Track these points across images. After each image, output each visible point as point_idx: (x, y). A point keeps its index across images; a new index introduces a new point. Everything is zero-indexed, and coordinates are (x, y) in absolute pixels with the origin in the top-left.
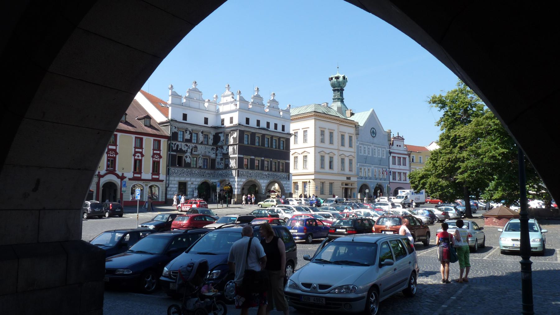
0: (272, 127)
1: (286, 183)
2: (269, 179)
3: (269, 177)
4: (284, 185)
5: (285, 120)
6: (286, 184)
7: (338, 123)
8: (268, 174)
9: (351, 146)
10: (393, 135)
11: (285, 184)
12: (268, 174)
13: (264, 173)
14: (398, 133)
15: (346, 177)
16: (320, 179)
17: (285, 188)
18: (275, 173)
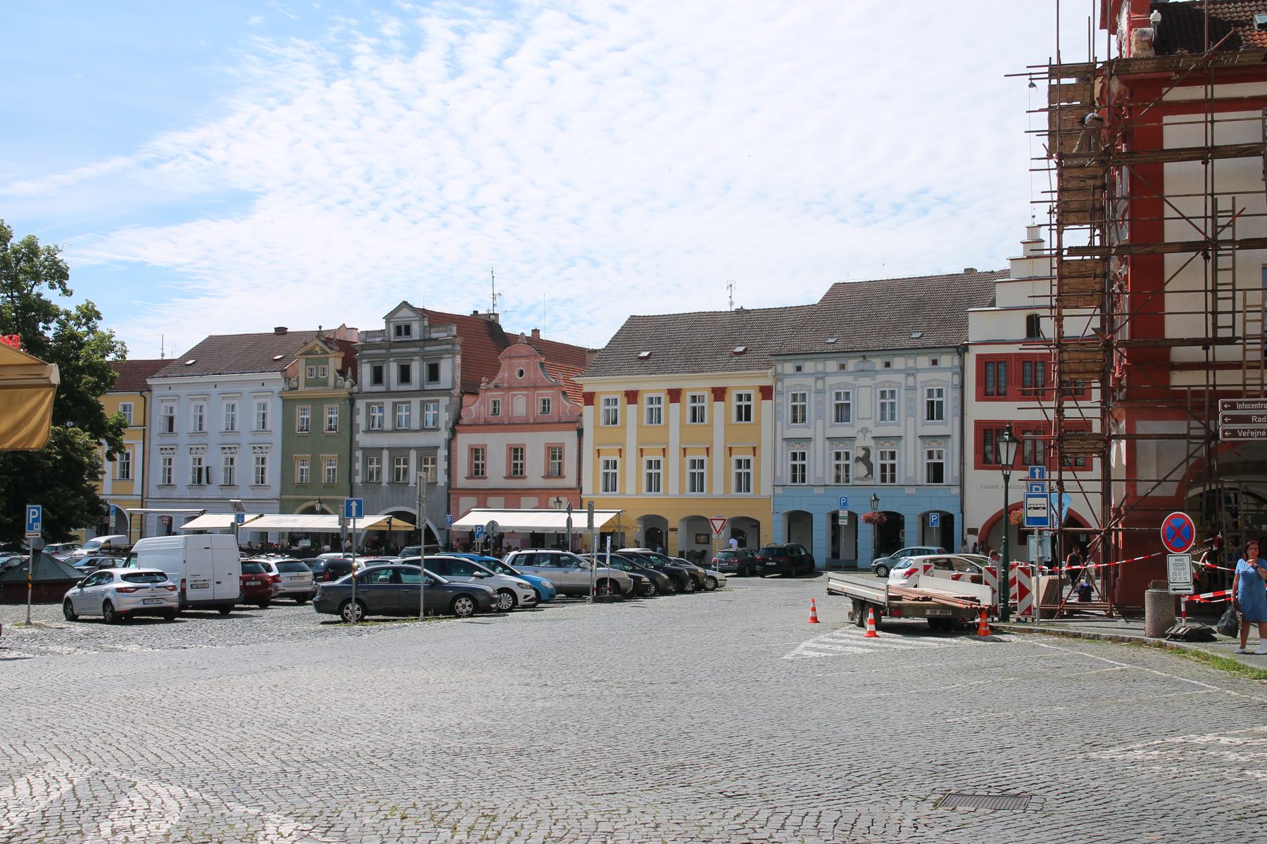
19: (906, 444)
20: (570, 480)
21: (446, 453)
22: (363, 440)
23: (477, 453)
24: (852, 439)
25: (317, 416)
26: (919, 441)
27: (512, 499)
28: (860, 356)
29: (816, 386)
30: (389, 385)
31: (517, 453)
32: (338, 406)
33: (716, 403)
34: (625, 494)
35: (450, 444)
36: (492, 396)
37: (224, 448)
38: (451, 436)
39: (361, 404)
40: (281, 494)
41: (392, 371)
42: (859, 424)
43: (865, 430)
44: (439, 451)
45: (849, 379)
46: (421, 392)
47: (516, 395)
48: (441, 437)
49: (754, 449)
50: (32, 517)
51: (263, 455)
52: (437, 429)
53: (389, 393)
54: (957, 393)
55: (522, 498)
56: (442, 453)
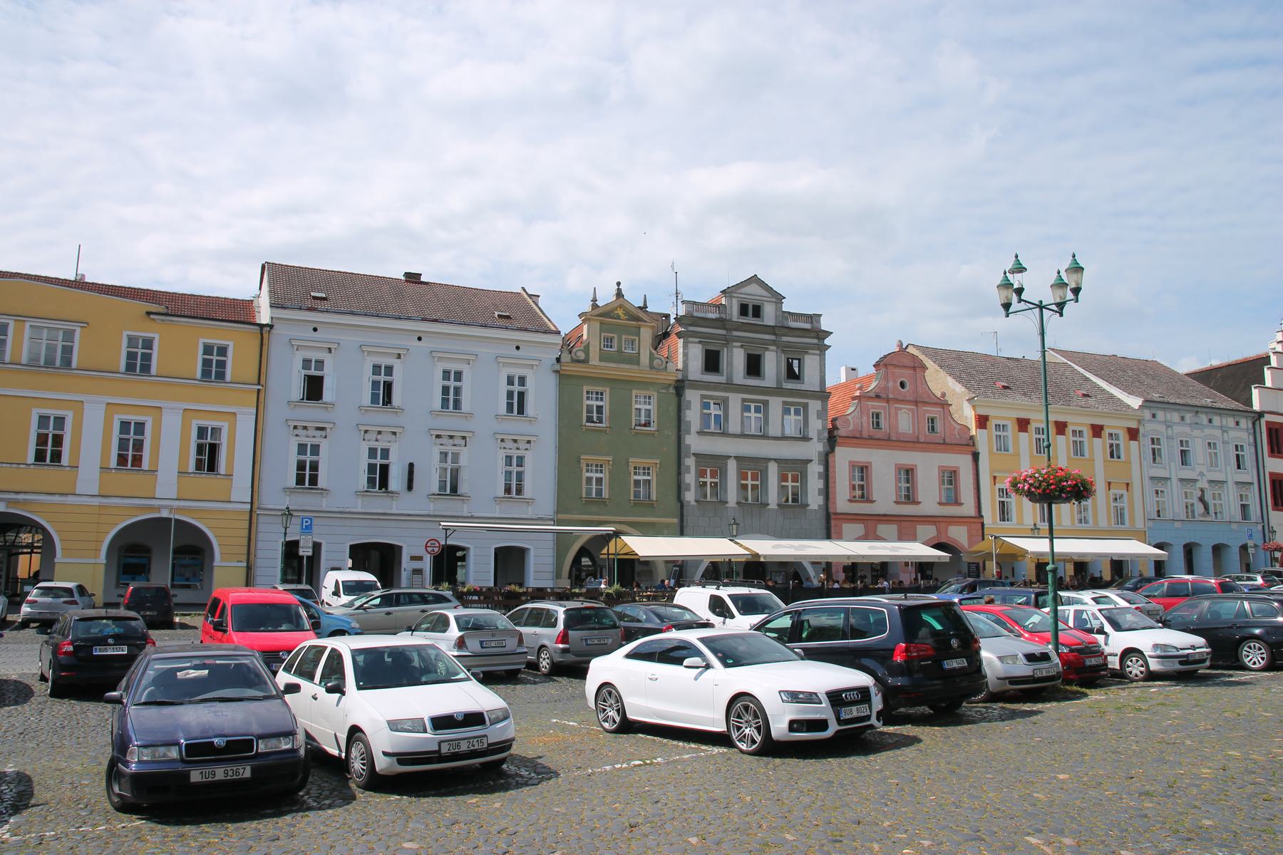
19: (1171, 485)
20: (968, 509)
21: (821, 469)
22: (694, 442)
23: (863, 470)
24: (1195, 481)
25: (621, 408)
26: (1235, 486)
27: (871, 526)
28: (1193, 411)
29: (1167, 433)
30: (730, 377)
31: (908, 473)
32: (655, 394)
33: (1131, 442)
34: (1022, 524)
35: (826, 459)
36: (873, 407)
37: (438, 436)
38: (828, 449)
39: (692, 396)
40: (558, 512)
41: (736, 360)
42: (1199, 469)
43: (1201, 474)
44: (809, 465)
45: (1187, 429)
46: (778, 391)
47: (900, 409)
48: (814, 448)
49: (1128, 484)
51: (520, 453)
52: (805, 439)
53: (730, 386)
54: (1253, 450)
55: (917, 526)
56: (815, 469)
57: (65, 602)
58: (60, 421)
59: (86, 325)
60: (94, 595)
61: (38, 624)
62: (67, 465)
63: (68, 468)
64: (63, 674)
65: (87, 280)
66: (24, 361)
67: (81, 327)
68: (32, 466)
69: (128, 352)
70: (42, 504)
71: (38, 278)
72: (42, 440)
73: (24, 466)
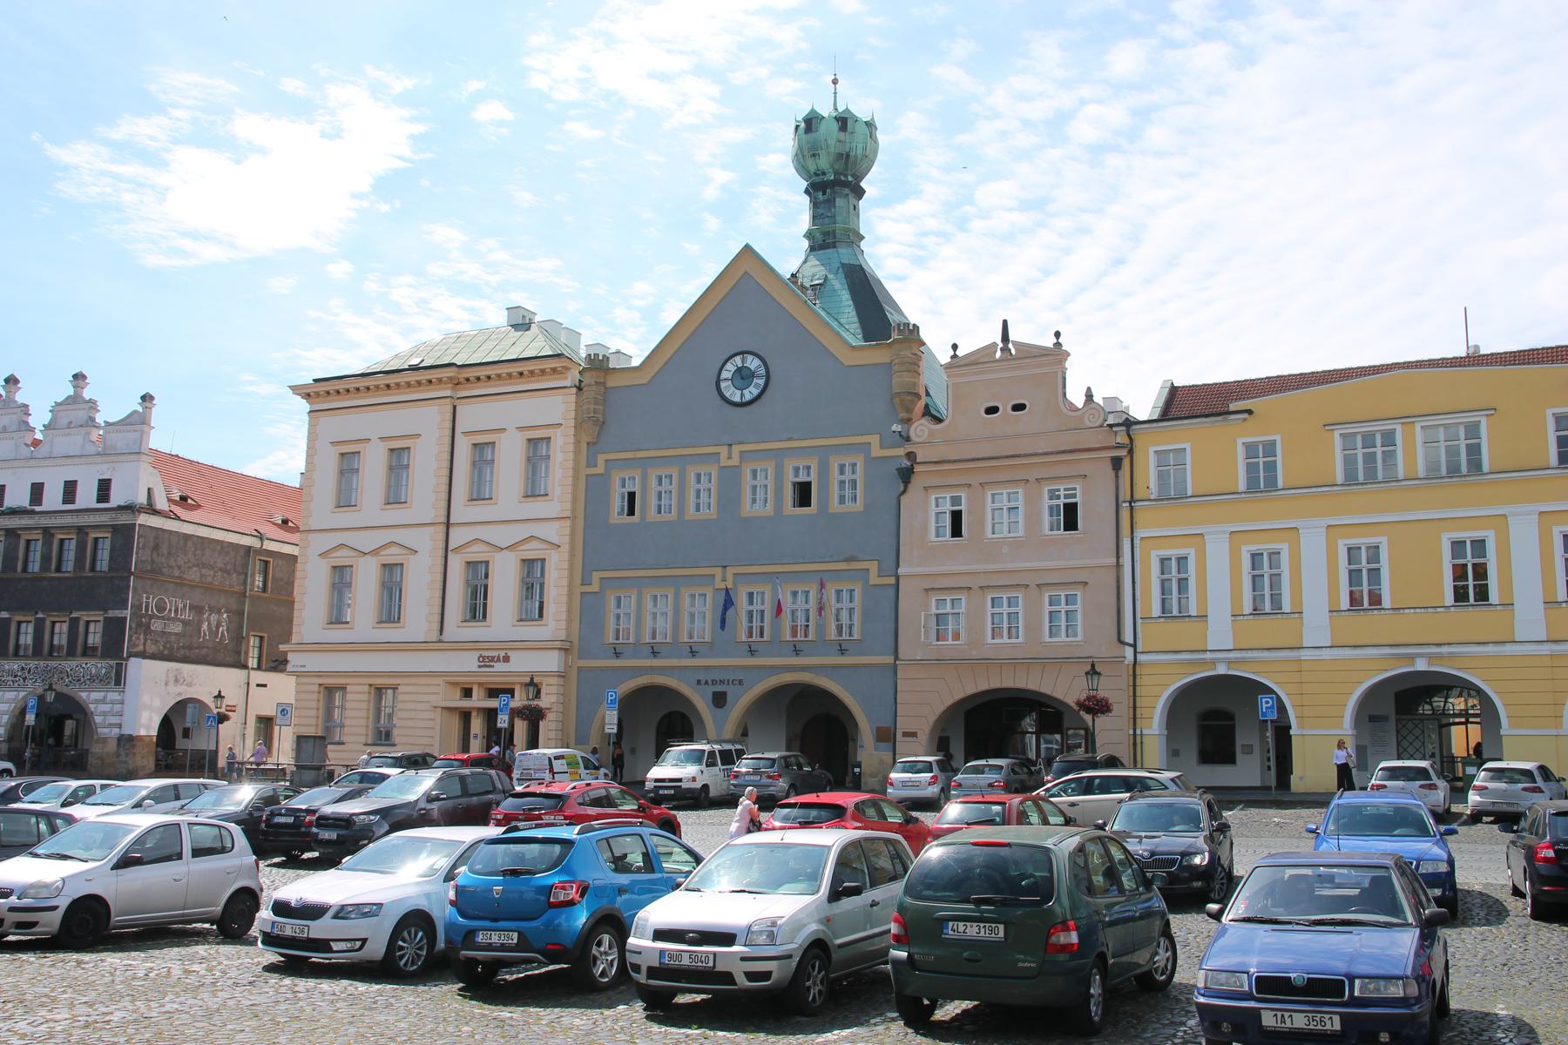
0: (53, 499)
1: (105, 697)
2: (25, 686)
3: (24, 679)
4: (92, 707)
5: (112, 458)
6: (103, 701)
7: (448, 393)
8: (23, 669)
9: (533, 492)
10: (955, 347)
11: (97, 702)
12: (23, 669)
13: (7, 667)
14: (1005, 323)
15: (477, 654)
16: (319, 674)
17: (98, 719)
18: (53, 663)
50: (1264, 705)
57: (1525, 789)
58: (1479, 545)
59: (1493, 412)
60: (1564, 780)
61: (1492, 818)
62: (1498, 603)
63: (1499, 608)
64: (1546, 888)
65: (1483, 351)
66: (1421, 473)
67: (1487, 415)
68: (1452, 609)
69: (1558, 437)
70: (1473, 657)
71: (1431, 363)
72: (1459, 573)
73: (1442, 610)
